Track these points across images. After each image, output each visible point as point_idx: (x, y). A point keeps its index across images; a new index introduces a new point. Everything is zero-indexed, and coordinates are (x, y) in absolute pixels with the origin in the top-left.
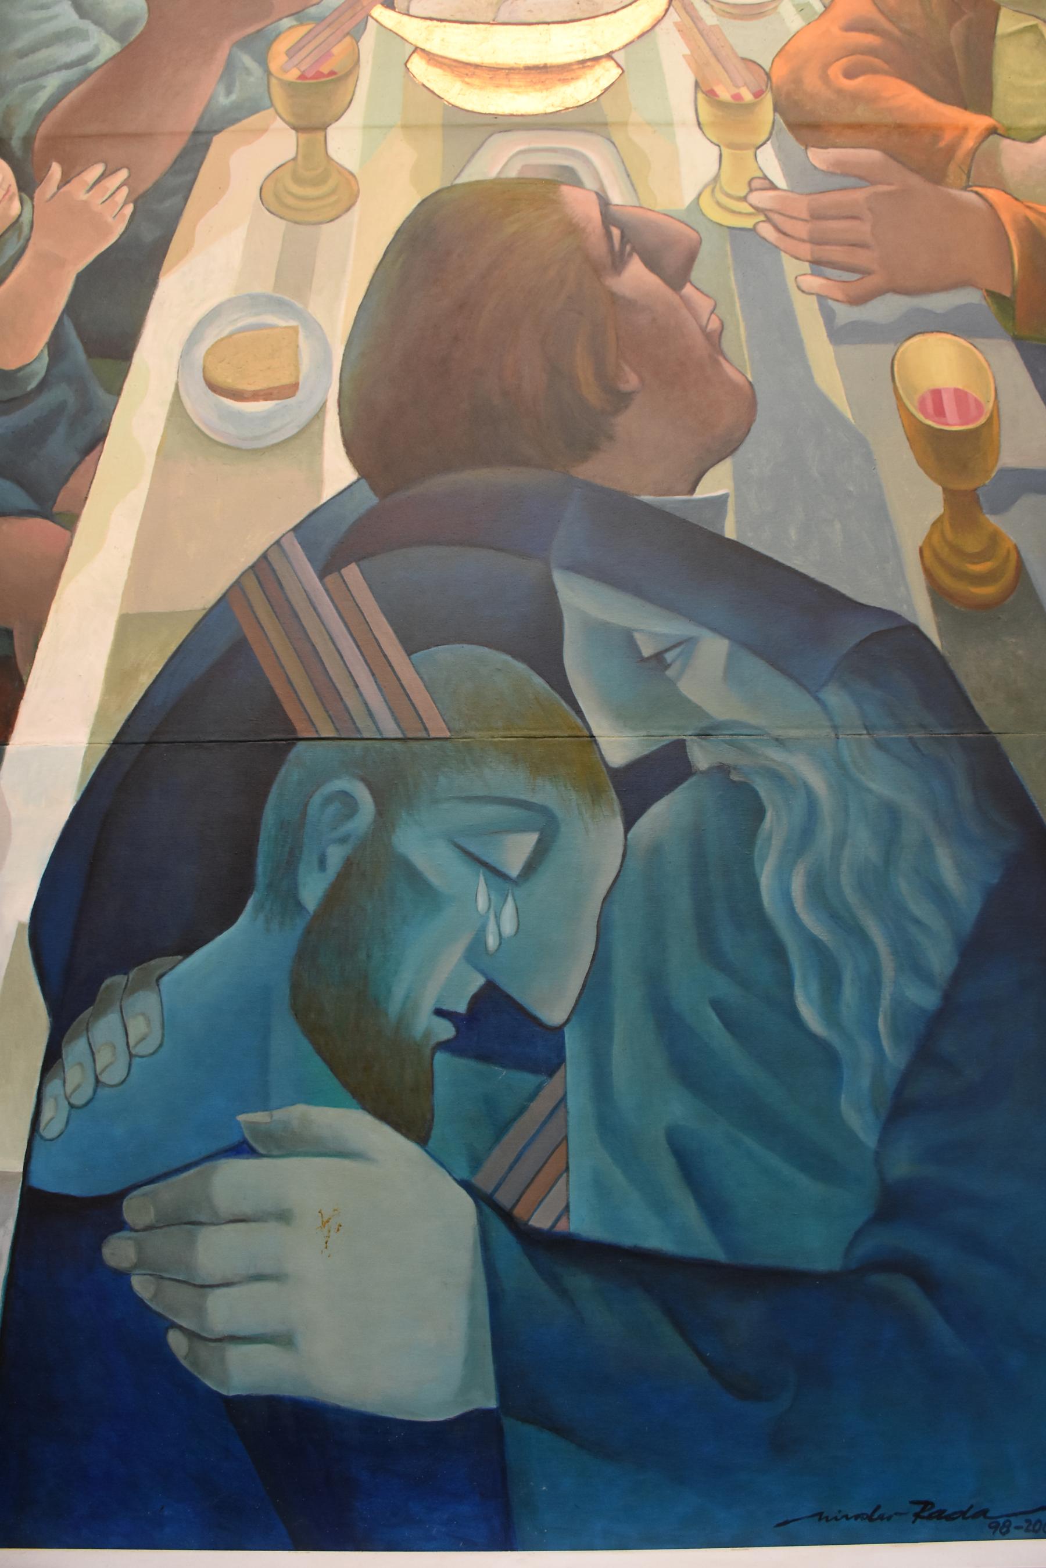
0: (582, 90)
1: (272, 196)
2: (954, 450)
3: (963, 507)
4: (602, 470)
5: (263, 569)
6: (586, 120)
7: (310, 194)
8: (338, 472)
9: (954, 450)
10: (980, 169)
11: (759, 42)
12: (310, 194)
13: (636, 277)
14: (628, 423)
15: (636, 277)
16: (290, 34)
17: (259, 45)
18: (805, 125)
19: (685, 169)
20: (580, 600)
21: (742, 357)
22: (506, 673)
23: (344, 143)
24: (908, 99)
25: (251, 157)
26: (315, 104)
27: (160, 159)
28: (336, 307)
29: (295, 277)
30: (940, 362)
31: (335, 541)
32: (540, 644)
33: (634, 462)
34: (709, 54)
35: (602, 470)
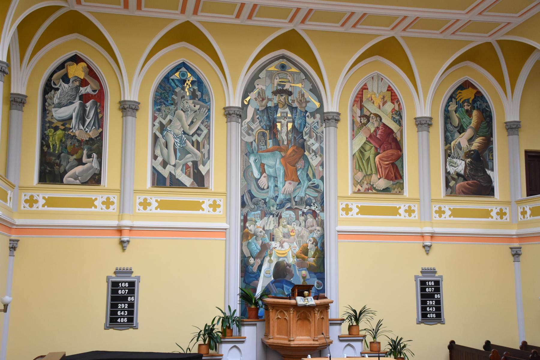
0: (285, 255)
1: (268, 262)
2: (304, 277)
3: (304, 281)
4: (286, 279)
5: (269, 284)
6: (285, 257)
7: (270, 261)
8: (273, 279)
9: (304, 277)
10: (307, 260)
11: (295, 252)
12: (270, 261)
13: (288, 267)
14: (288, 276)
15: (288, 267)
16: (269, 251)
17: (267, 251)
18: (297, 257)
19: (291, 260)
20: (285, 286)
21: (293, 272)
22: (281, 290)
23: (272, 258)
24: (303, 256)
25: (267, 259)
26: (271, 255)
27: (262, 259)
28: (272, 269)
29: (270, 267)
30: (304, 272)
31: (273, 282)
32: (283, 289)
33: (287, 278)
34: (292, 252)
35: (286, 279)
